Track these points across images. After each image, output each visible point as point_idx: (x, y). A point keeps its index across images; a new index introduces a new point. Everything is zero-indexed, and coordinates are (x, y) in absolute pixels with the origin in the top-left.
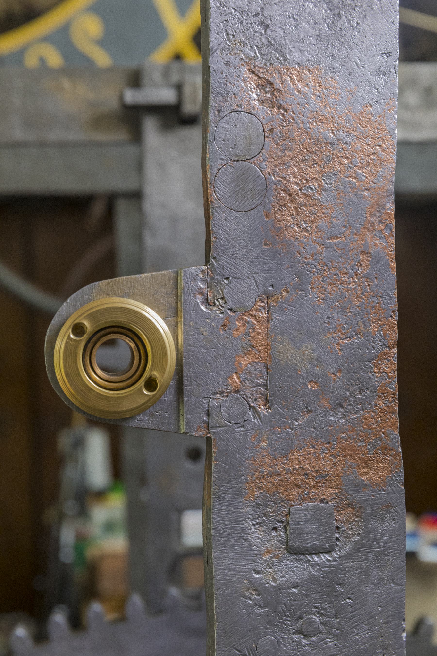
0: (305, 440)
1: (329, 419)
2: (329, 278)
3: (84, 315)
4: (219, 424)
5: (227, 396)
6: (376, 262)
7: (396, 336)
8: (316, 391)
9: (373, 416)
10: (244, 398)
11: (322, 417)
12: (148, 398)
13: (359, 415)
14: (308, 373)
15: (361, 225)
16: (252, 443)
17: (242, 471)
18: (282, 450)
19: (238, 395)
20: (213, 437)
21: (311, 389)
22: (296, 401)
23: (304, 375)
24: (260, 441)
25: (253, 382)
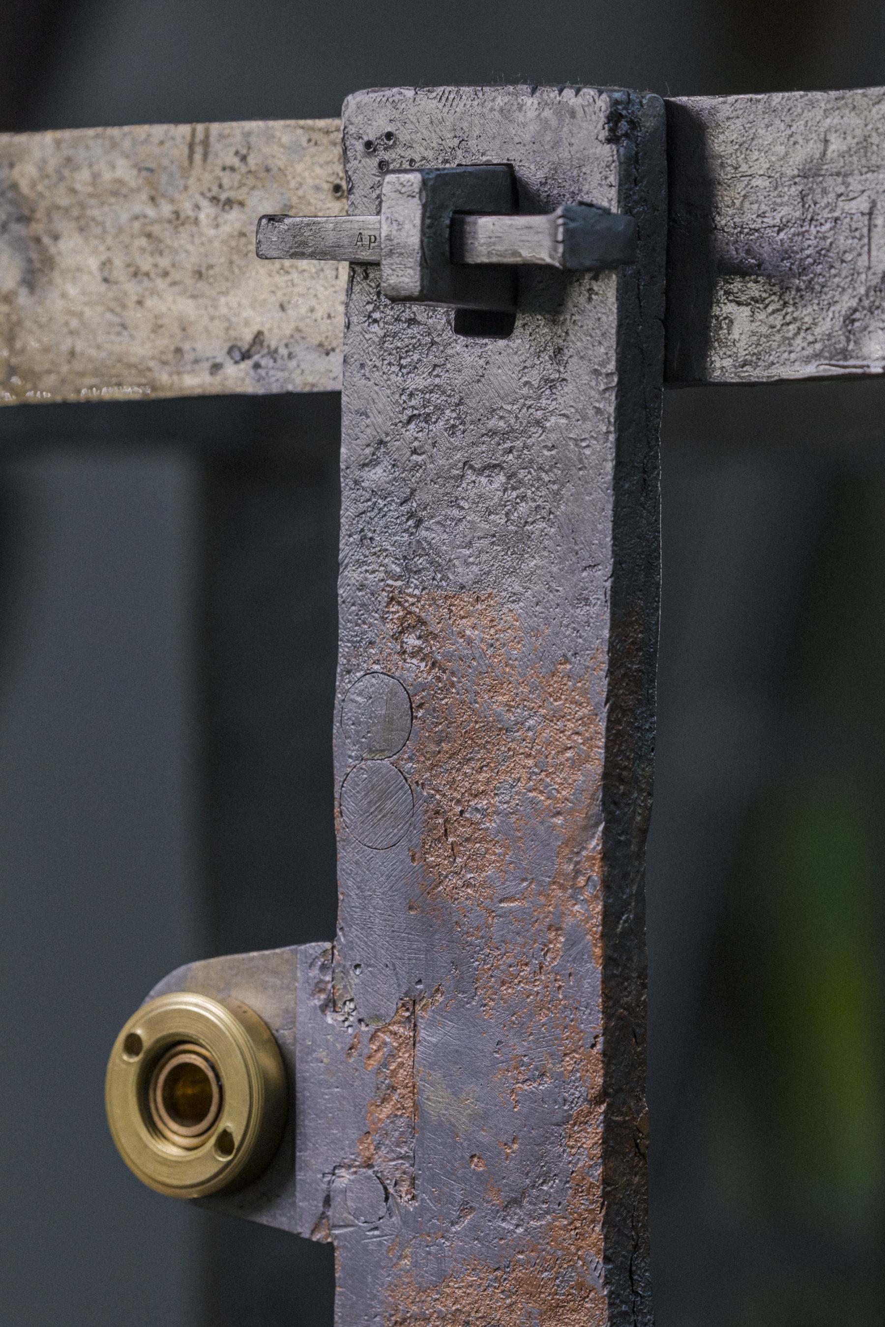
0: (465, 1259)
1: (499, 1226)
2: (502, 972)
3: (143, 1020)
4: (343, 1221)
5: (355, 1173)
6: (572, 945)
7: (600, 1081)
8: (481, 1174)
9: (565, 1226)
10: (378, 1178)
11: (490, 1221)
12: (221, 1166)
13: (544, 1223)
14: (470, 1140)
15: (549, 877)
16: (390, 1258)
17: (375, 1307)
18: (432, 1275)
19: (370, 1172)
20: (336, 1243)
21: (474, 1170)
22: (453, 1190)
23: (465, 1144)
24: (400, 1258)
25: (393, 1151)
